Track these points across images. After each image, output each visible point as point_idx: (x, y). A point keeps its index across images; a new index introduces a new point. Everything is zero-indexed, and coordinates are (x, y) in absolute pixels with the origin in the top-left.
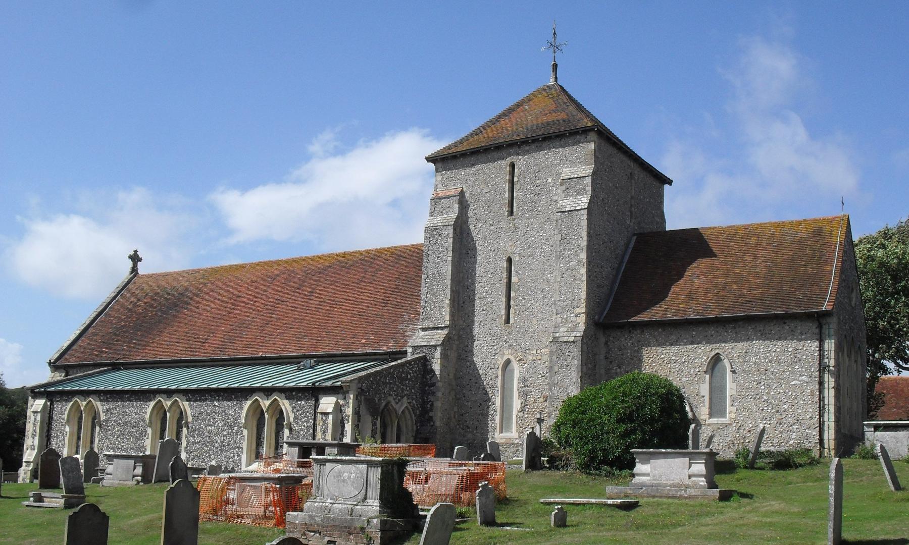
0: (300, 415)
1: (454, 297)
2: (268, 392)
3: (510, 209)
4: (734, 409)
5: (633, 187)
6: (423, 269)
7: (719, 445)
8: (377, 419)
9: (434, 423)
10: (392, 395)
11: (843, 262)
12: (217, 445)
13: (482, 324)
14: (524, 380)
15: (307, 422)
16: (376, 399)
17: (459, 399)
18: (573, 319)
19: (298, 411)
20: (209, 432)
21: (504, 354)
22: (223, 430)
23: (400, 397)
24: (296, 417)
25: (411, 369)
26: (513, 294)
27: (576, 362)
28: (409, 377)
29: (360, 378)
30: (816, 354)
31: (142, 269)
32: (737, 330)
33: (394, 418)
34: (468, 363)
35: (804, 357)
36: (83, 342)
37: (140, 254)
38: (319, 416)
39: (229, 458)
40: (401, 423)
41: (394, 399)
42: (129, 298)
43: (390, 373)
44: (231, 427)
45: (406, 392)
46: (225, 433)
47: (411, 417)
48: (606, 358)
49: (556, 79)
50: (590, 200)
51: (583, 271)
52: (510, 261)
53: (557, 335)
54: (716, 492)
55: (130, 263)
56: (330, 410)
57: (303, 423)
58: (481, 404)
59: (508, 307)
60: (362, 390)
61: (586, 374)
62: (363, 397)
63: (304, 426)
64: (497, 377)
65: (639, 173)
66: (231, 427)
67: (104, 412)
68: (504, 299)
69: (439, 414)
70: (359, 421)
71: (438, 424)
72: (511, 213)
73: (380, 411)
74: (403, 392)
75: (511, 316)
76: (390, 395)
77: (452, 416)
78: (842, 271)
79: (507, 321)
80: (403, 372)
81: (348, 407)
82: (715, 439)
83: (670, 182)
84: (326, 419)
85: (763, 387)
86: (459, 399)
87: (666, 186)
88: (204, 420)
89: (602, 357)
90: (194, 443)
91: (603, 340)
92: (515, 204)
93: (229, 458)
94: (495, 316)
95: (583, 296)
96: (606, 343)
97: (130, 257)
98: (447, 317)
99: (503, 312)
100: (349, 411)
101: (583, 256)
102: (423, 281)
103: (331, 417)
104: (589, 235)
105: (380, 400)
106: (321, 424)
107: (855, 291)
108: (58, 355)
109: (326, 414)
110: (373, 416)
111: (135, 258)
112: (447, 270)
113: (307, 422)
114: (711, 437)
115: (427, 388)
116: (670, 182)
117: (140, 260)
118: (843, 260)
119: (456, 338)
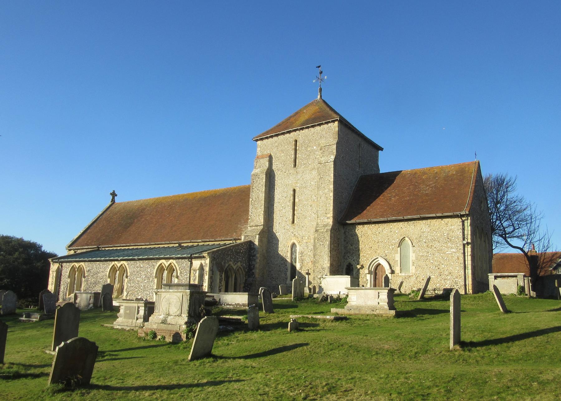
0: (183, 271)
1: (266, 210)
2: (167, 259)
3: (294, 164)
5: (360, 152)
6: (251, 196)
7: (406, 287)
8: (222, 273)
9: (255, 276)
10: (232, 261)
11: (475, 186)
12: (141, 288)
13: (280, 224)
14: (302, 253)
15: (186, 275)
16: (223, 263)
17: (268, 263)
19: (182, 269)
20: (138, 282)
21: (291, 239)
22: (144, 280)
23: (236, 262)
24: (181, 273)
25: (242, 248)
26: (296, 208)
27: (328, 243)
28: (241, 251)
29: (213, 252)
30: (460, 237)
31: (117, 200)
33: (233, 273)
34: (273, 245)
35: (453, 238)
36: (85, 236)
37: (116, 193)
38: (192, 271)
39: (147, 295)
40: (237, 276)
41: (233, 263)
42: (109, 215)
43: (230, 249)
44: (149, 278)
45: (239, 260)
46: (146, 281)
47: (243, 273)
48: (345, 241)
49: (321, 96)
50: (335, 157)
51: (332, 194)
52: (294, 191)
53: (318, 228)
54: (393, 312)
55: (111, 197)
56: (198, 268)
57: (184, 275)
58: (280, 266)
59: (294, 215)
60: (214, 258)
61: (333, 249)
62: (215, 262)
63: (185, 277)
64: (288, 252)
65: (365, 145)
66: (149, 278)
67: (87, 271)
68: (291, 211)
69: (257, 271)
70: (213, 274)
71: (257, 276)
72: (295, 165)
73: (225, 269)
74: (238, 259)
75: (295, 219)
76: (230, 261)
77: (265, 272)
78: (475, 191)
79: (293, 222)
80: (238, 249)
81: (207, 267)
82: (404, 284)
83: (382, 149)
84: (195, 273)
85: (430, 255)
86: (268, 263)
87: (380, 152)
88: (135, 275)
89: (343, 240)
92: (297, 161)
93: (147, 295)
94: (286, 220)
95: (332, 208)
96: (345, 233)
97: (111, 194)
98: (262, 221)
99: (291, 217)
100: (207, 269)
101: (332, 187)
102: (250, 202)
103: (198, 271)
104: (334, 175)
105: (225, 263)
106: (193, 276)
107: (483, 203)
108: (71, 243)
109: (195, 270)
110: (220, 272)
111: (114, 195)
112: (262, 196)
113: (186, 275)
114: (402, 283)
115: (251, 257)
116: (382, 149)
117: (116, 195)
118: (475, 185)
119: (267, 231)
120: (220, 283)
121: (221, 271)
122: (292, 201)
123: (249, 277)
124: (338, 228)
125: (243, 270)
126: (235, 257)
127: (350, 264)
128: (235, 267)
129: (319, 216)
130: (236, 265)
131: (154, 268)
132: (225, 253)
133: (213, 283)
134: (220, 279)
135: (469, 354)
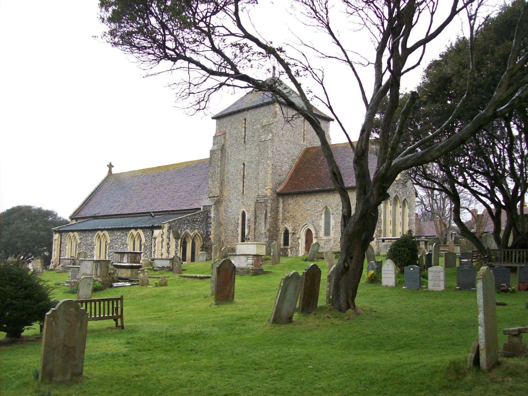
4: (333, 232)
5: (305, 126)
15: (150, 242)
18: (265, 192)
21: (241, 208)
22: (121, 246)
32: (335, 194)
37: (113, 164)
46: (121, 247)
47: (200, 238)
48: (283, 209)
52: (244, 164)
53: (258, 199)
55: (108, 169)
71: (212, 241)
73: (181, 236)
75: (244, 190)
76: (187, 229)
80: (195, 218)
90: (111, 252)
91: (281, 200)
111: (110, 166)
113: (150, 242)
117: (113, 167)
120: (176, 248)
121: (177, 237)
122: (242, 174)
123: (206, 242)
124: (277, 198)
125: (200, 236)
126: (192, 225)
127: (286, 229)
128: (191, 234)
129: (260, 188)
130: (193, 233)
131: (127, 236)
132: (181, 222)
133: (170, 249)
134: (176, 245)
135: (372, 306)
